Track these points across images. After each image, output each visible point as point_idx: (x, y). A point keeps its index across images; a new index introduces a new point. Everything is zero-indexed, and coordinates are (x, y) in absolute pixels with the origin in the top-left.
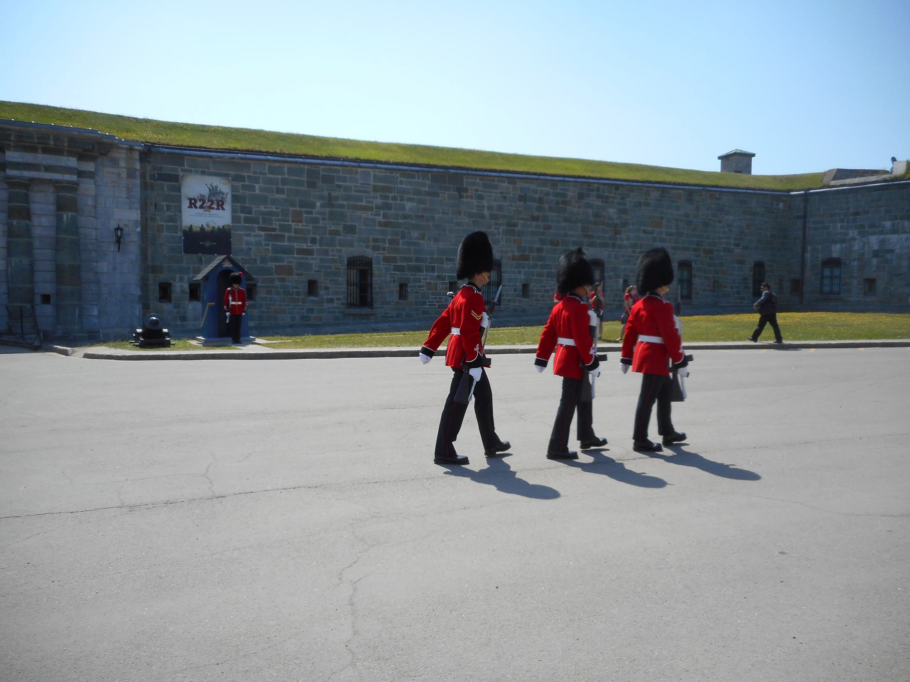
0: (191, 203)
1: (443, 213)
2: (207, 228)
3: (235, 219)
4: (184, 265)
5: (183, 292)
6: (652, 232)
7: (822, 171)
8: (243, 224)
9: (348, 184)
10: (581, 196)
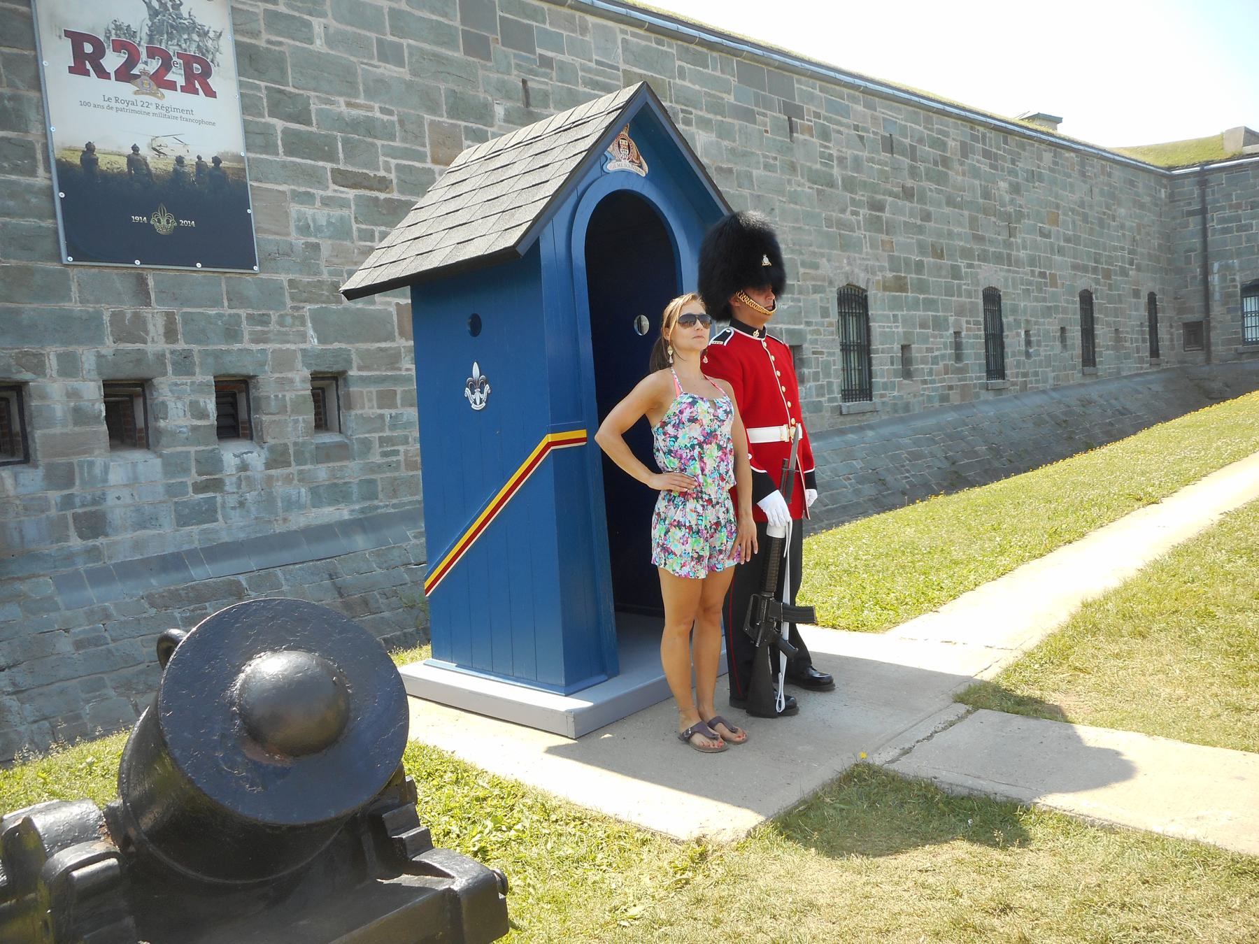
0: (78, 54)
1: (767, 167)
2: (156, 165)
3: (255, 136)
4: (74, 305)
5: (80, 416)
6: (1048, 236)
7: (1218, 132)
8: (282, 157)
9: (566, 58)
10: (965, 150)
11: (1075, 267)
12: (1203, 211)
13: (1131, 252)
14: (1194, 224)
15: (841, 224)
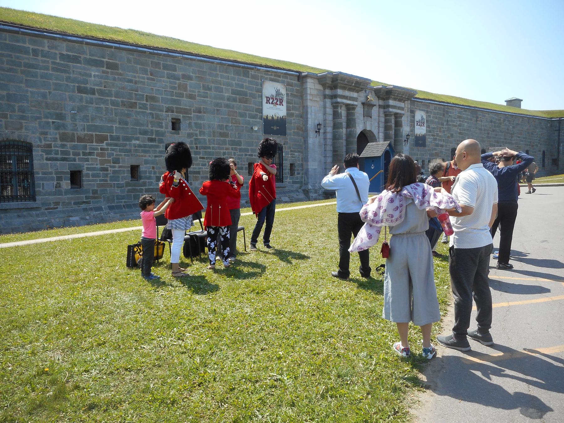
10: (504, 120)
11: (525, 145)
12: (559, 130)
13: (539, 140)
14: (556, 133)
15: (483, 138)
